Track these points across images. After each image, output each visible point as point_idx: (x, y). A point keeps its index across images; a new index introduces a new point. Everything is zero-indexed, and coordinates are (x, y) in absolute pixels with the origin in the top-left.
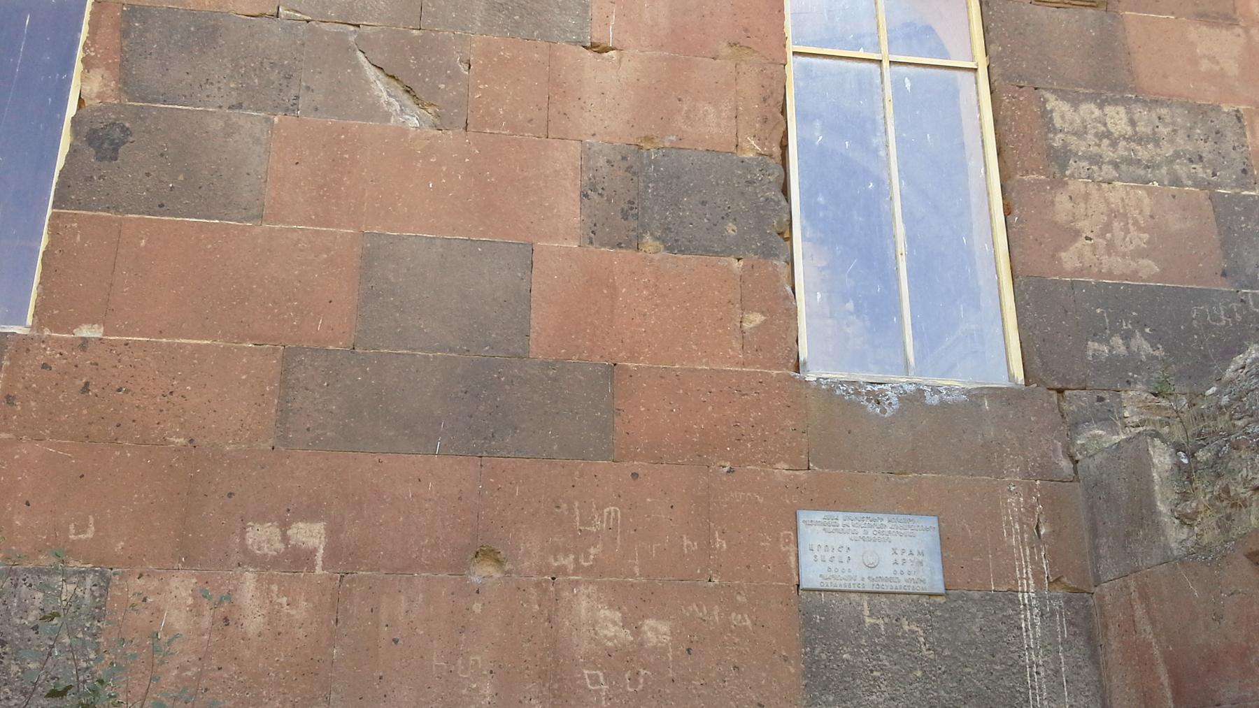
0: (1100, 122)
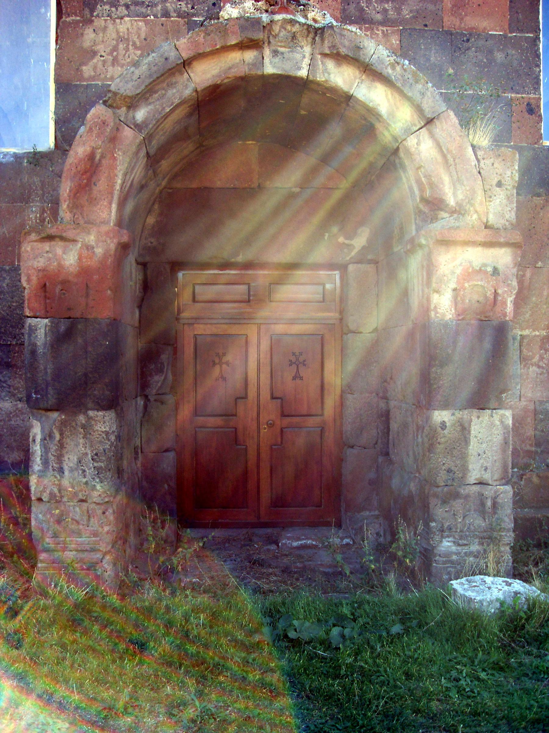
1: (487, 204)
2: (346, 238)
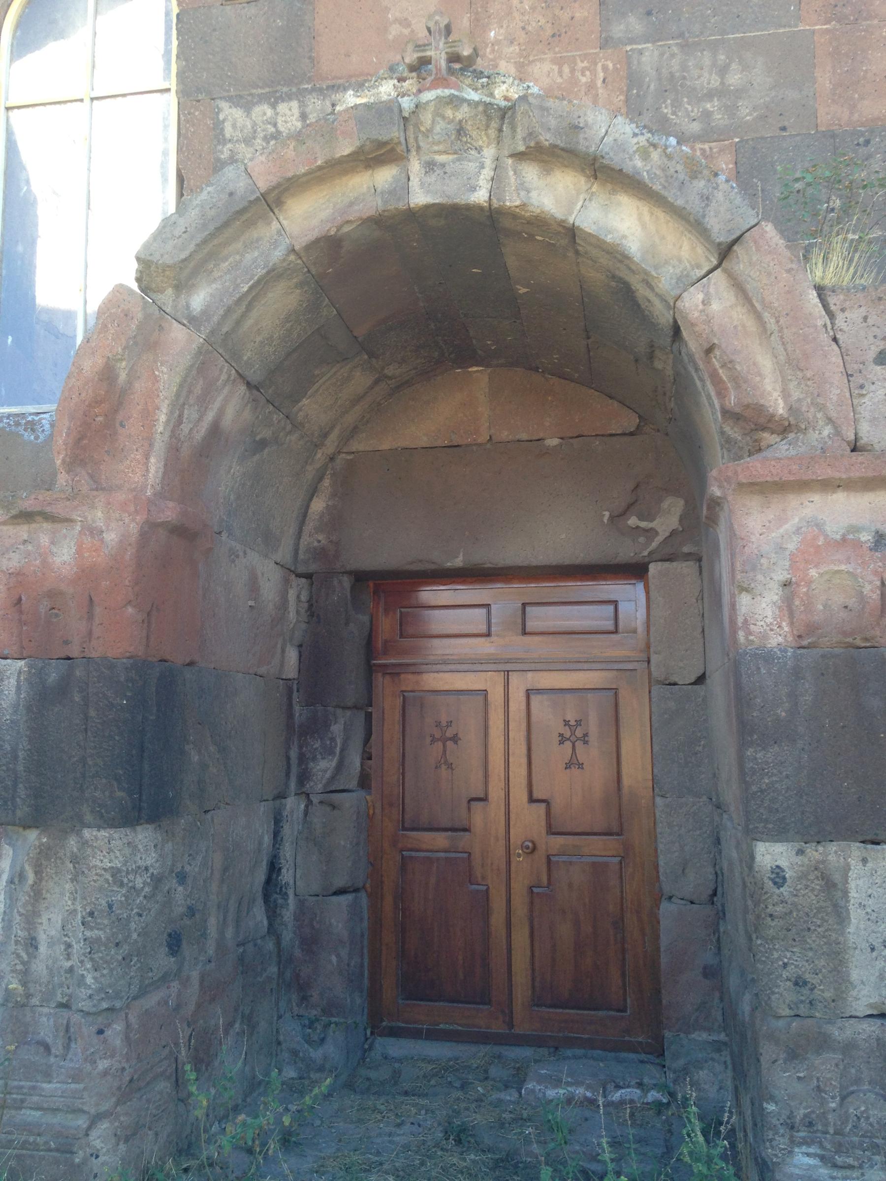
0: (270, 123)
1: (856, 402)
2: (641, 518)
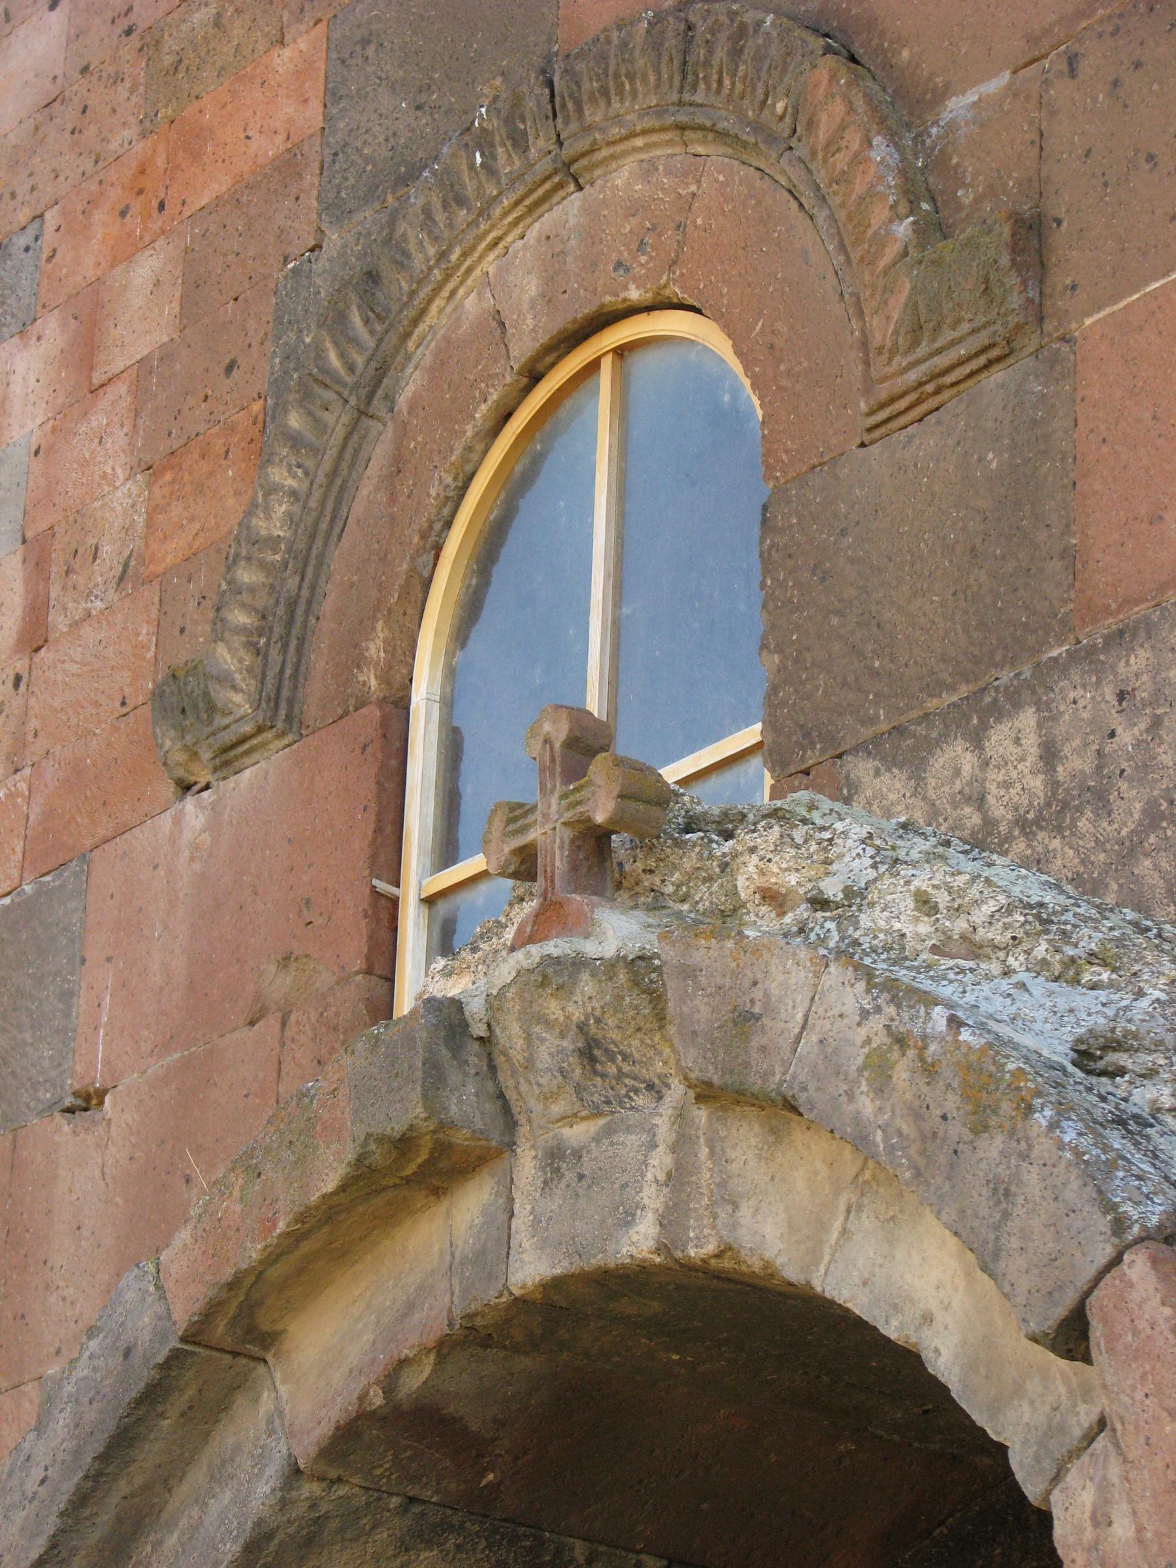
0: (968, 800)
